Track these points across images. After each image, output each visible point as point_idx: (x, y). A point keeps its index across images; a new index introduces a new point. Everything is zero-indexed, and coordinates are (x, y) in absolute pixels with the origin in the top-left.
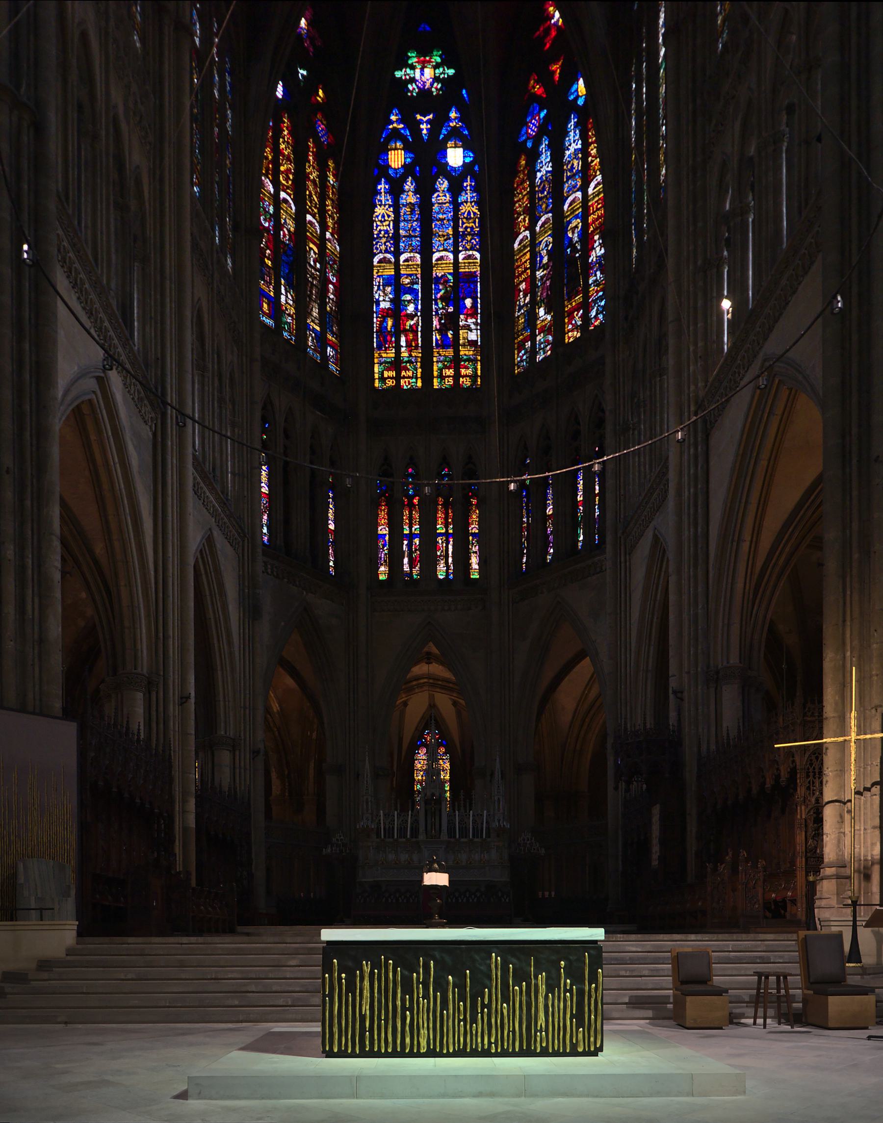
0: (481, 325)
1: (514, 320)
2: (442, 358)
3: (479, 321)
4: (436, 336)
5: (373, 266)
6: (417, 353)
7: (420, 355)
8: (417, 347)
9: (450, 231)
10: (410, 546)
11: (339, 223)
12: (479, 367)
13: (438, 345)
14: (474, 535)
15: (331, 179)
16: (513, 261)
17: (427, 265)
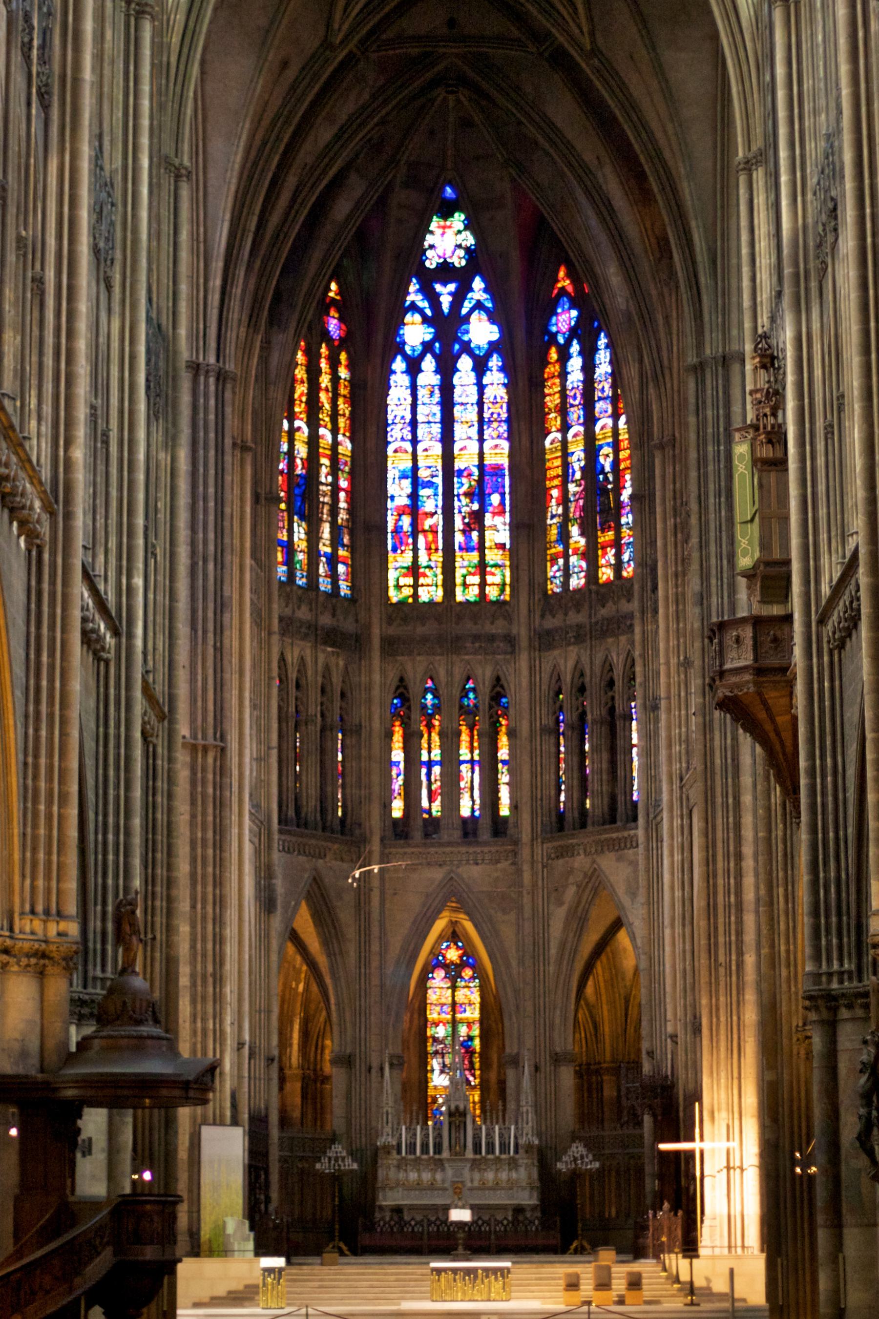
0: (510, 524)
1: (545, 529)
2: (466, 563)
3: (508, 520)
4: (459, 538)
5: (386, 457)
6: (438, 557)
7: (441, 559)
8: (437, 550)
9: (475, 418)
10: (429, 774)
11: (352, 418)
12: (508, 572)
13: (461, 549)
14: (504, 762)
15: (343, 373)
16: (543, 461)
17: (448, 457)
